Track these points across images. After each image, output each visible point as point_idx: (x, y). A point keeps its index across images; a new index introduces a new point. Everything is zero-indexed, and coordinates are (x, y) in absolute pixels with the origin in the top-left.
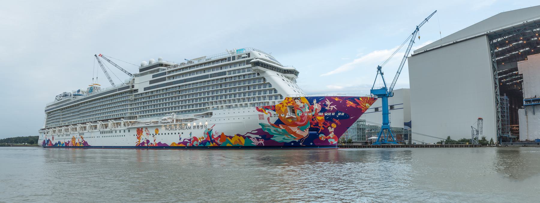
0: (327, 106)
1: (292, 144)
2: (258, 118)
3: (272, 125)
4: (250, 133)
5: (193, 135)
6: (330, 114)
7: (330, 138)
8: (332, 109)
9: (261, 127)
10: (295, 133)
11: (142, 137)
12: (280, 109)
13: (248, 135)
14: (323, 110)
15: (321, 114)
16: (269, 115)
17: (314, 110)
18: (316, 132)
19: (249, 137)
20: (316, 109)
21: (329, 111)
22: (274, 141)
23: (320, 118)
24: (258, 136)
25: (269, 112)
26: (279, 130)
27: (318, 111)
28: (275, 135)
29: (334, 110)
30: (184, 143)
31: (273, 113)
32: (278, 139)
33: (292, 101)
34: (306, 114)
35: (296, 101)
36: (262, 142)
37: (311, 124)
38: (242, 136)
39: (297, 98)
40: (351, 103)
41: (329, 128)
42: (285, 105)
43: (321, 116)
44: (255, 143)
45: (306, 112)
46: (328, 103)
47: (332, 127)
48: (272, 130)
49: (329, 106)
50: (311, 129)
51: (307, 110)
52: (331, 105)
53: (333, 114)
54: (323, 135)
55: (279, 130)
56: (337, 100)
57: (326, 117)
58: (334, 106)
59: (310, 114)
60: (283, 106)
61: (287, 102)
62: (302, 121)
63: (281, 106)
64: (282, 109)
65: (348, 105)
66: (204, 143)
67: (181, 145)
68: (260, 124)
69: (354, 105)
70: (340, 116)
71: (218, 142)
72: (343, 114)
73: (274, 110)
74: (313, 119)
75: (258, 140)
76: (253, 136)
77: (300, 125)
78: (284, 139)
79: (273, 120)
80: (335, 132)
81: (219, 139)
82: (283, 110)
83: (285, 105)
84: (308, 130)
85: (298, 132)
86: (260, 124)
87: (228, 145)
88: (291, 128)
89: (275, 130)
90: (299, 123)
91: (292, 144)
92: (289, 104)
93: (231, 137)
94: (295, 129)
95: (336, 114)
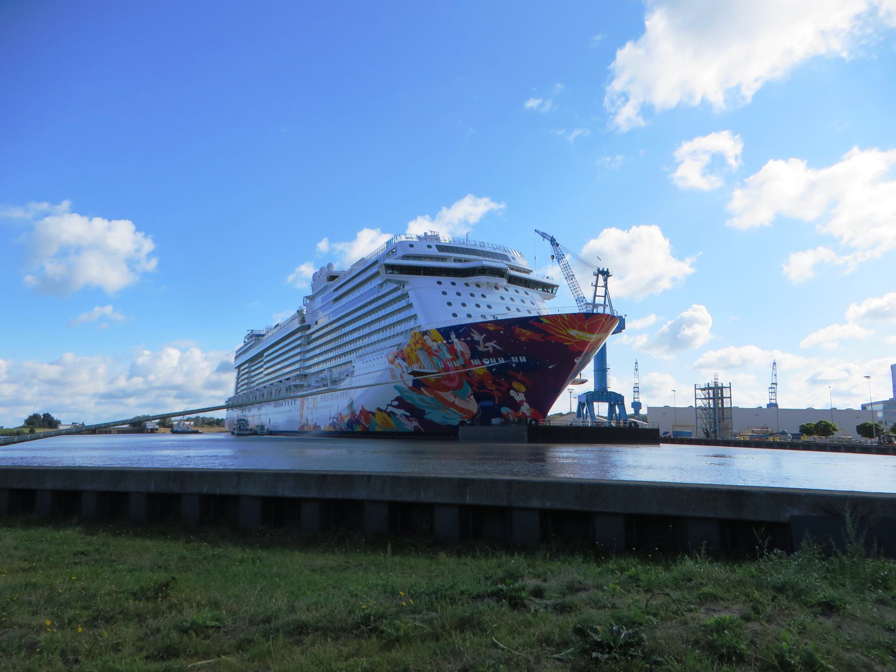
0: (478, 343)
3: (410, 388)
4: (391, 405)
6: (494, 362)
8: (491, 349)
9: (398, 394)
10: (453, 404)
13: (390, 409)
14: (476, 354)
15: (476, 362)
17: (459, 354)
19: (395, 414)
20: (462, 353)
22: (431, 423)
24: (403, 412)
26: (425, 398)
27: (468, 356)
28: (427, 410)
30: (333, 425)
32: (436, 416)
33: (420, 339)
34: (450, 365)
35: (426, 337)
36: (417, 424)
37: (471, 385)
38: (385, 411)
39: (425, 333)
40: (529, 333)
44: (411, 425)
46: (477, 337)
47: (517, 391)
48: (415, 398)
49: (481, 342)
51: (449, 357)
52: (485, 341)
54: (508, 410)
55: (429, 400)
56: (491, 329)
58: (492, 344)
59: (457, 364)
60: (411, 350)
61: (414, 340)
63: (409, 349)
65: (523, 339)
66: (350, 424)
67: (332, 429)
69: (537, 337)
70: (519, 364)
72: (523, 359)
73: (404, 359)
78: (443, 417)
79: (409, 380)
80: (530, 398)
82: (413, 357)
83: (414, 347)
84: (472, 397)
85: (457, 402)
86: (395, 387)
87: (378, 429)
89: (422, 400)
90: (447, 383)
94: (449, 396)
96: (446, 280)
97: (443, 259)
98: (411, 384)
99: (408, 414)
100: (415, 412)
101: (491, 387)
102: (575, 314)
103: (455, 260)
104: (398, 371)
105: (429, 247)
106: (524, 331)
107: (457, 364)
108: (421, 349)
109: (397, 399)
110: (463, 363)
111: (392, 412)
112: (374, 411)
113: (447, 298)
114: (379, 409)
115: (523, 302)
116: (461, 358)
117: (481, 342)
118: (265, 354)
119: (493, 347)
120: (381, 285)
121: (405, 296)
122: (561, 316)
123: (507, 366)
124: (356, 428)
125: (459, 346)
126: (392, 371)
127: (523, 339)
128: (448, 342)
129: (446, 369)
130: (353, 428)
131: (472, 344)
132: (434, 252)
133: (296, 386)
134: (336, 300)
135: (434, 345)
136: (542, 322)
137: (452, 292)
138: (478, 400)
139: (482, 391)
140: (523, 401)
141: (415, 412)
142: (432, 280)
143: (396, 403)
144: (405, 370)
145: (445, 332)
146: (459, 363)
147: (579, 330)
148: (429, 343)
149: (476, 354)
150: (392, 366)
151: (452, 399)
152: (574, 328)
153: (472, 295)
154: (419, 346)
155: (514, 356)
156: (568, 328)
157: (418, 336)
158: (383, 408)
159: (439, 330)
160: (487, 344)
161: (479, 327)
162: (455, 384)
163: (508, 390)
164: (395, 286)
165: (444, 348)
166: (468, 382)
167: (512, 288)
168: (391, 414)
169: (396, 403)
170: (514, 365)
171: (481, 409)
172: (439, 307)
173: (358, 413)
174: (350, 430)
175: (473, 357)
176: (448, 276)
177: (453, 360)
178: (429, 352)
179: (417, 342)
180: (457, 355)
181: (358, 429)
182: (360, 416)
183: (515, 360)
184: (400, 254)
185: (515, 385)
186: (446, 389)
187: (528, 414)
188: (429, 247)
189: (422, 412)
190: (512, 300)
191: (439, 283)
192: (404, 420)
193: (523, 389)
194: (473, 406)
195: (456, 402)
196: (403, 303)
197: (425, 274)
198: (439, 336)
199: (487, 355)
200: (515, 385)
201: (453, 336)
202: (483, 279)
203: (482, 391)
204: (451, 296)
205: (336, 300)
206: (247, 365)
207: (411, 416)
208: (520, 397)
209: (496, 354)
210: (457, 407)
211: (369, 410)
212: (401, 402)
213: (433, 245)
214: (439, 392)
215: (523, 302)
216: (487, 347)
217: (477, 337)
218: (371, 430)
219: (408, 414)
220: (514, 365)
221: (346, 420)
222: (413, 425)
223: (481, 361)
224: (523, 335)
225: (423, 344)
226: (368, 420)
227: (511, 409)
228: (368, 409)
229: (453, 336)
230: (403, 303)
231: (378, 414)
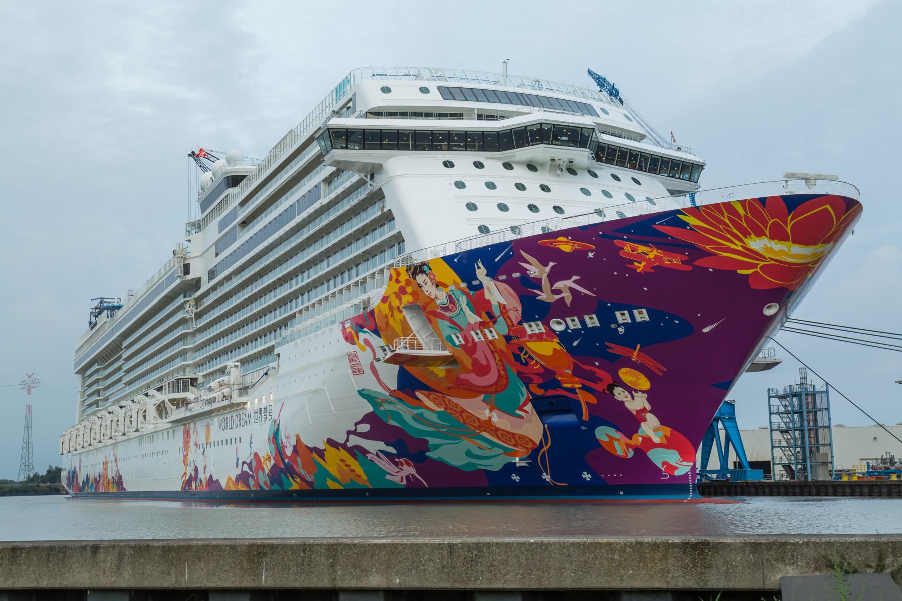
1: (516, 478)
2: (350, 371)
3: (392, 393)
4: (355, 433)
5: (254, 450)
6: (574, 323)
7: (648, 441)
8: (568, 297)
9: (370, 409)
10: (487, 425)
11: (194, 455)
12: (388, 323)
13: (354, 441)
14: (534, 309)
15: (534, 328)
16: (368, 348)
17: (496, 312)
18: (571, 418)
19: (365, 452)
20: (502, 307)
21: (559, 309)
22: (441, 465)
23: (546, 348)
24: (381, 445)
25: (366, 341)
27: (515, 315)
28: (432, 441)
29: (579, 306)
31: (377, 342)
32: (452, 453)
33: (408, 283)
35: (421, 279)
36: (412, 471)
37: (527, 382)
38: (344, 446)
39: (419, 269)
40: (653, 254)
41: (620, 394)
42: (396, 303)
43: (539, 337)
45: (472, 327)
46: (534, 269)
47: (630, 389)
48: (405, 415)
49: (545, 283)
50: (544, 407)
52: (554, 277)
53: (593, 321)
54: (612, 432)
55: (434, 417)
56: (567, 248)
57: (565, 337)
58: (569, 283)
60: (391, 308)
61: (396, 287)
62: (481, 369)
63: (385, 308)
64: (391, 320)
65: (641, 267)
67: (241, 487)
68: (363, 393)
69: (673, 261)
71: (303, 472)
72: (642, 316)
73: (376, 332)
74: (517, 358)
75: (397, 464)
76: (373, 446)
77: (484, 390)
78: (469, 453)
79: (390, 375)
81: (299, 460)
83: (396, 303)
84: (529, 407)
85: (497, 419)
86: (363, 393)
87: (332, 485)
88: (464, 403)
91: (516, 478)
92: (407, 299)
93: (321, 453)
94: (478, 408)
95: (607, 317)
96: (463, 160)
97: (455, 115)
98: (394, 386)
99: (394, 451)
100: (409, 447)
101: (570, 382)
102: (763, 201)
103: (480, 117)
104: (365, 357)
105: (425, 90)
106: (642, 249)
107: (494, 334)
108: (411, 307)
109: (367, 419)
110: (505, 332)
111: (357, 447)
112: (322, 447)
113: (468, 195)
114: (330, 442)
115: (629, 197)
116: (501, 320)
117: (545, 283)
118: (125, 343)
119: (571, 289)
120: (328, 181)
121: (378, 196)
122: (728, 206)
123: (607, 330)
124: (290, 481)
125: (496, 293)
126: (352, 357)
127: (641, 267)
128: (471, 287)
129: (470, 347)
130: (281, 484)
131: (525, 288)
132: (435, 100)
133: (177, 403)
134: (244, 224)
135: (441, 297)
136: (684, 225)
137: (475, 181)
138: (542, 413)
139: (551, 392)
140: (644, 410)
141: (409, 447)
142: (432, 160)
143: (365, 428)
144: (380, 354)
145: (463, 264)
146: (494, 334)
147: (772, 238)
148: (429, 290)
149: (534, 309)
150: (351, 348)
151: (485, 413)
152: (760, 234)
153: (520, 187)
154: (407, 299)
155: (621, 308)
156: (746, 234)
157: (404, 277)
158: (341, 440)
159: (448, 260)
160: (559, 285)
161: (540, 246)
162: (490, 379)
163: (611, 388)
164: (356, 178)
165: (463, 301)
166: (520, 374)
167: (605, 171)
168: (357, 452)
169: (365, 428)
170: (621, 330)
171: (553, 431)
172: (443, 209)
173: (289, 452)
174: (276, 487)
175: (527, 316)
176: (466, 148)
177: (482, 324)
178: (430, 312)
179: (403, 291)
180: (491, 315)
181: (295, 485)
182: (293, 458)
183: (623, 317)
184: (362, 108)
185: (626, 374)
186: (472, 391)
187: (657, 440)
188: (425, 90)
189: (423, 446)
190: (607, 194)
191: (448, 164)
192: (385, 465)
193: (644, 383)
194: (532, 428)
195: (495, 419)
196: (374, 213)
197: (416, 148)
198: (448, 275)
199: (559, 309)
200: (626, 374)
201: (481, 273)
202: (538, 152)
203: (551, 392)
204: (475, 189)
205: (244, 224)
206: (95, 367)
207: (399, 455)
208: (637, 403)
209: (579, 306)
210: (496, 431)
211: (311, 446)
212: (377, 425)
213: (433, 86)
214: (455, 400)
215: (629, 197)
216: (558, 292)
217: (534, 269)
218: (316, 487)
219: (394, 451)
220: (621, 330)
221: (268, 466)
222: (404, 474)
223: (546, 324)
224: (642, 257)
225: (414, 294)
226: (310, 466)
227: (618, 429)
228: (309, 441)
229: (481, 273)
230: (374, 213)
231: (330, 451)
